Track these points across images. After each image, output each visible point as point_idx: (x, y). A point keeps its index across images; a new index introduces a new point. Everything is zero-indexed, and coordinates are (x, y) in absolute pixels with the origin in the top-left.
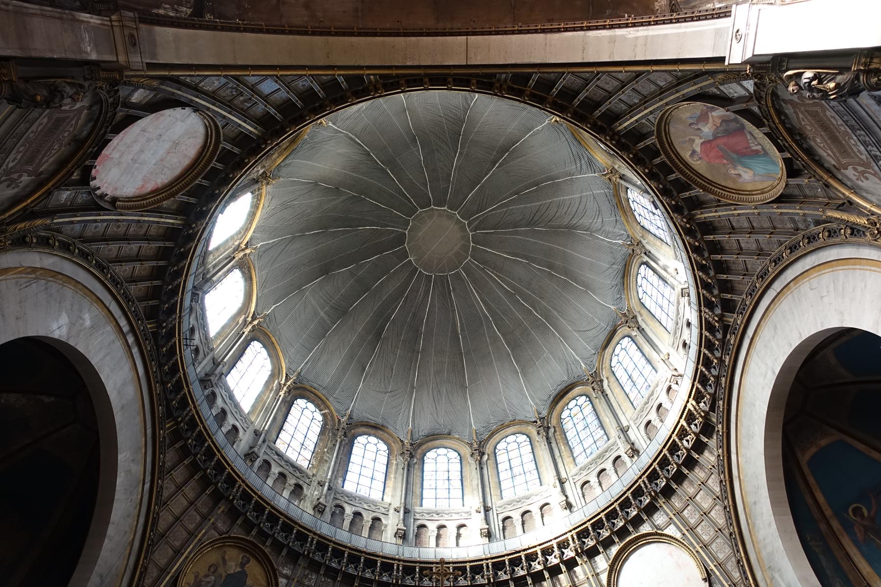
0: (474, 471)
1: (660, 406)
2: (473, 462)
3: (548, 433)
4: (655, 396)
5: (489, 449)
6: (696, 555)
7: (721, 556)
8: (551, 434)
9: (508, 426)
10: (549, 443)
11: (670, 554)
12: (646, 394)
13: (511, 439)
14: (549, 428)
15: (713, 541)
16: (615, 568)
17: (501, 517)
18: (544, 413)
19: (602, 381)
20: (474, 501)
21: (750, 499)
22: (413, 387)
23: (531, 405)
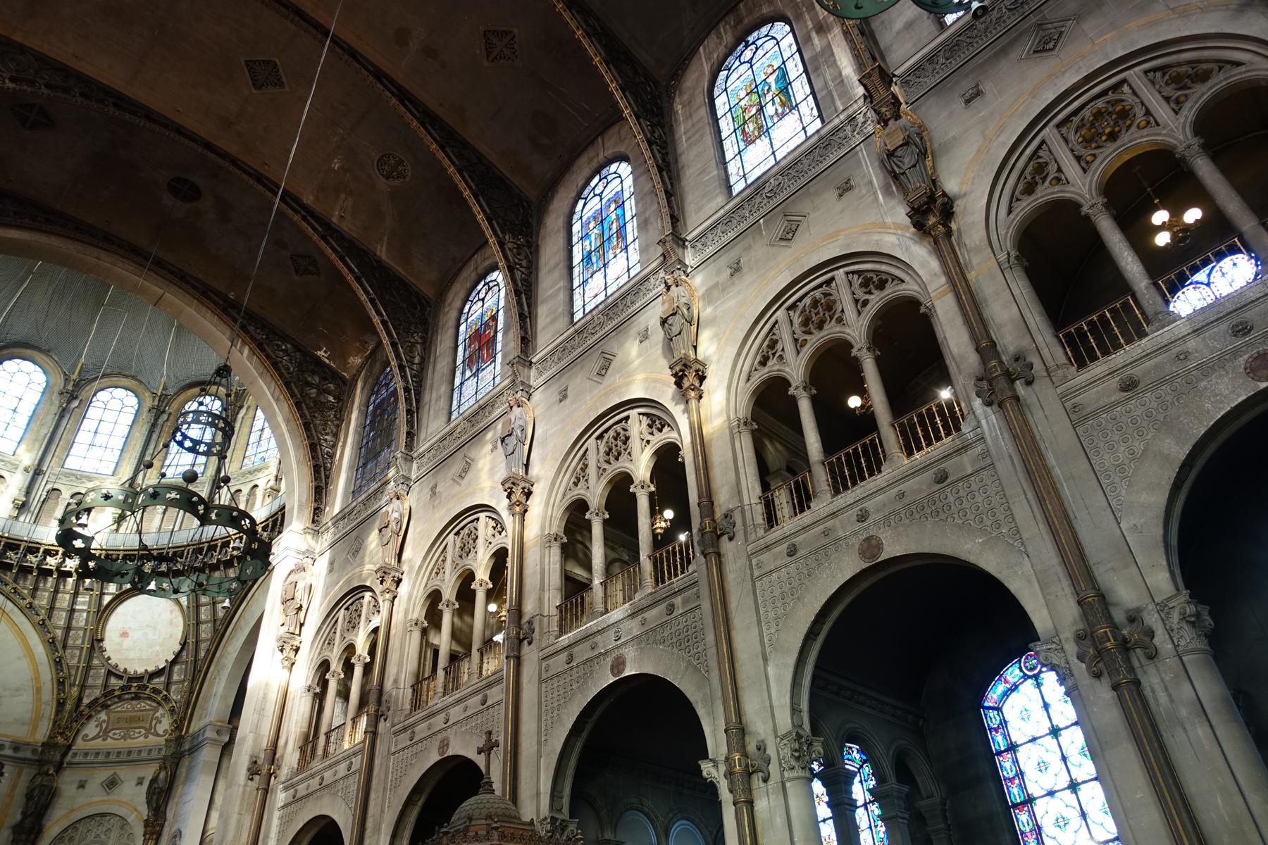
0: (51, 416)
1: (256, 486)
2: (57, 402)
3: (156, 419)
4: (260, 475)
5: (83, 394)
6: (187, 627)
7: (203, 636)
8: (160, 421)
9: (126, 376)
10: (151, 432)
11: (171, 612)
12: (258, 463)
13: (120, 392)
14: (164, 412)
15: (206, 622)
16: (120, 598)
17: (49, 486)
18: (171, 391)
19: (241, 407)
20: (27, 458)
21: (242, 622)
22: (30, 272)
23: (163, 378)
